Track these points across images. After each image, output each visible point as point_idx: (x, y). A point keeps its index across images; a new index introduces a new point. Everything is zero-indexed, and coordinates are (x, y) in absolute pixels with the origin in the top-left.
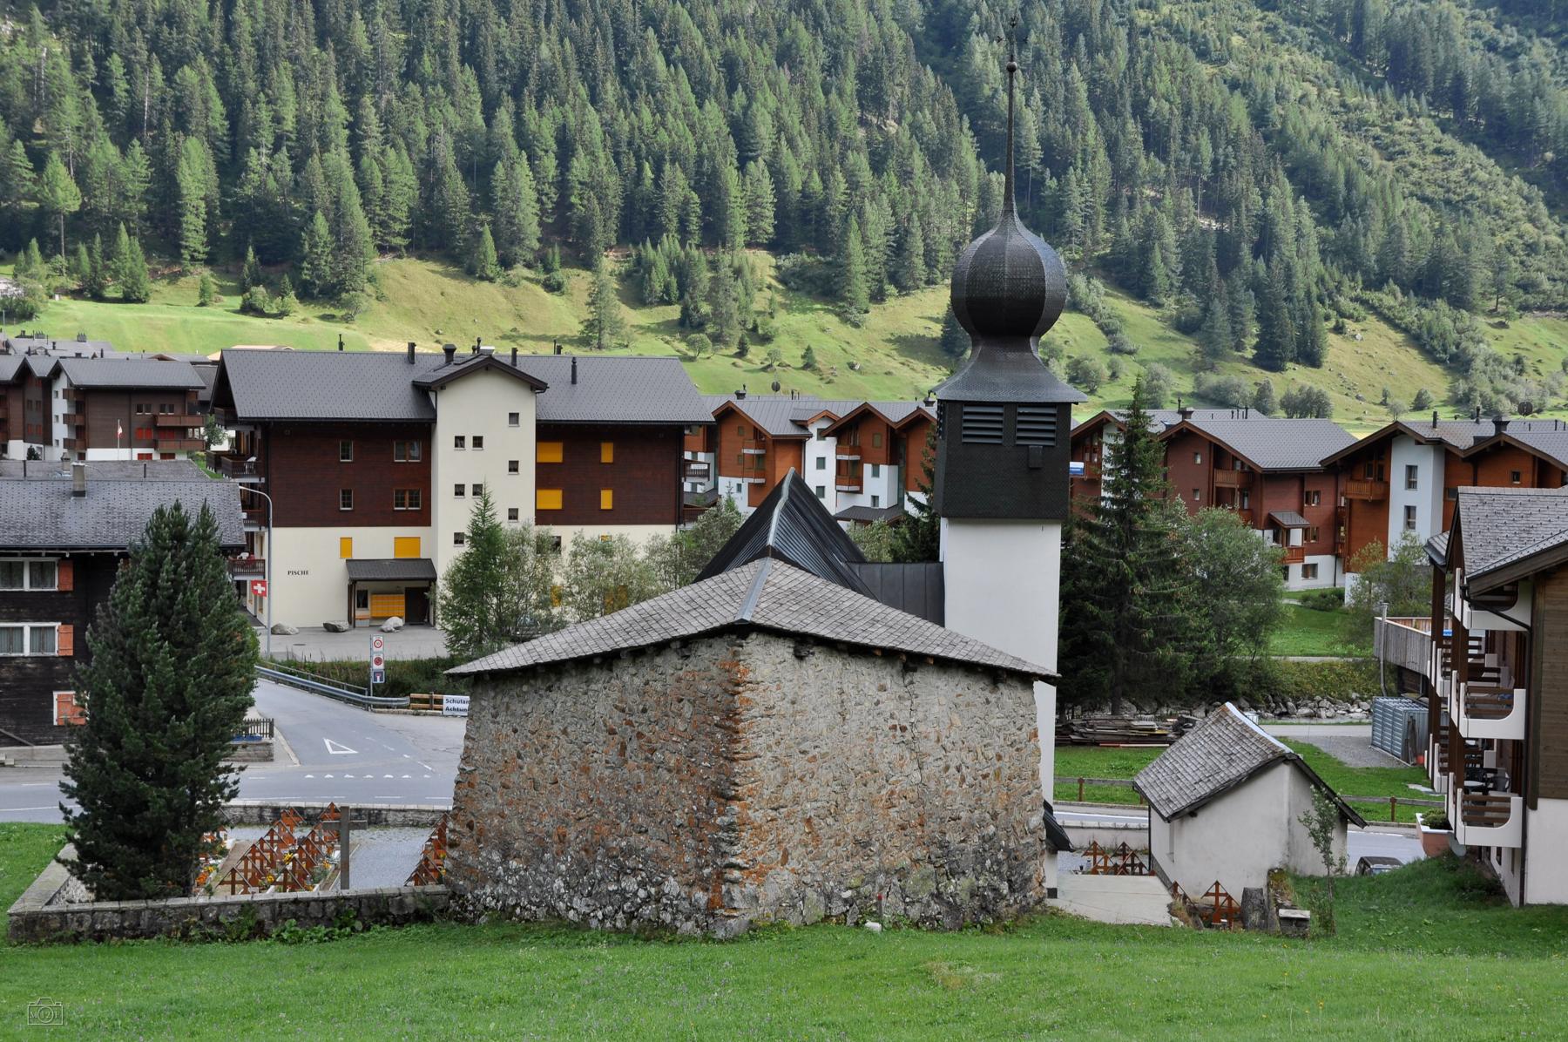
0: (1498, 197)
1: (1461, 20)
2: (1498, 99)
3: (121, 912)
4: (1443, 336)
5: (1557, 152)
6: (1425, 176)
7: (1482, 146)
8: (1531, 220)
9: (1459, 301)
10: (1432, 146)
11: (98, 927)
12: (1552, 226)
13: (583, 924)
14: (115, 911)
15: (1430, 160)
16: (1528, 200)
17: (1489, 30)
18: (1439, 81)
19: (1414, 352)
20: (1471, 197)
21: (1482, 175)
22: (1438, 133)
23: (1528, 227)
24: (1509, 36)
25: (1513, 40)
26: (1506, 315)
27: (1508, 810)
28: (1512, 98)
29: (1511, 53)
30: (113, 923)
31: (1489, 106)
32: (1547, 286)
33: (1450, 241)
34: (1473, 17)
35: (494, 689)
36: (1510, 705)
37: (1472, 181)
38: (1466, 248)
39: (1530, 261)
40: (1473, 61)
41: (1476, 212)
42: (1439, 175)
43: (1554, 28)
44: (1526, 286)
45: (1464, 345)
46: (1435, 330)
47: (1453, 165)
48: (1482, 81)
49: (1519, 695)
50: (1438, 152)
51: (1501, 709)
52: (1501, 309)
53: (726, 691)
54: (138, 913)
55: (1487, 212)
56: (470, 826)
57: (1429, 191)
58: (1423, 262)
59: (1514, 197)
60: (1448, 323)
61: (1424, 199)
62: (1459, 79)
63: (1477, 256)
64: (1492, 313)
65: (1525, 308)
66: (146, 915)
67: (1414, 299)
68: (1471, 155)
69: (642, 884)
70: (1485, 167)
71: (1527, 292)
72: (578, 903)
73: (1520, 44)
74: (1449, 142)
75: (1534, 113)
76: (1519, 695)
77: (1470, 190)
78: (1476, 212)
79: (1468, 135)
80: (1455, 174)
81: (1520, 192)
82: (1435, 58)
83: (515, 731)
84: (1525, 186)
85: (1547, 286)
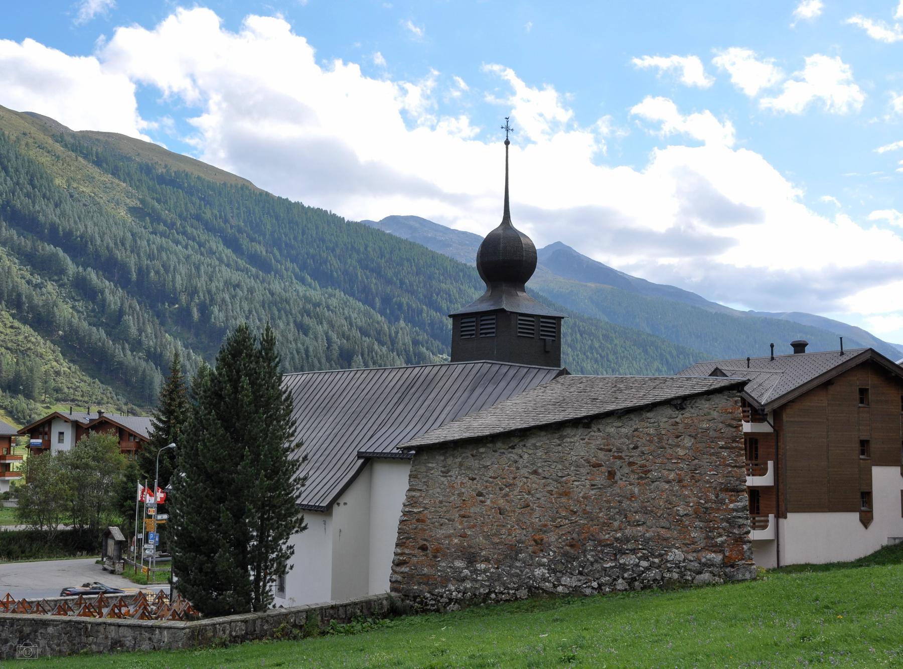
0: (41, 350)
1: (15, 270)
2: (37, 306)
3: (245, 621)
4: (23, 412)
5: (64, 331)
6: (7, 337)
7: (31, 326)
8: (56, 361)
9: (29, 396)
10: (9, 325)
11: (234, 634)
12: (65, 364)
13: (576, 593)
14: (242, 621)
15: (8, 331)
16: (54, 352)
17: (28, 276)
18: (10, 295)
19: (10, 419)
20: (29, 349)
21: (33, 340)
22: (11, 319)
23: (55, 364)
24: (37, 279)
25: (39, 281)
26: (50, 403)
27: (768, 521)
28: (43, 306)
29: (37, 286)
30: (241, 630)
31: (33, 308)
32: (66, 390)
33: (22, 368)
34: (20, 269)
35: (444, 454)
36: (767, 470)
37: (29, 341)
38: (31, 371)
39: (58, 379)
40: (24, 287)
41: (33, 357)
42: (13, 338)
43: (56, 278)
44: (58, 390)
45: (33, 416)
46: (19, 409)
47: (19, 333)
48: (29, 297)
49: (770, 464)
50: (12, 327)
51: (763, 472)
52: (47, 400)
53: (730, 425)
54: (254, 621)
55: (37, 356)
56: (424, 548)
57: (9, 345)
58: (11, 377)
59: (48, 350)
60: (24, 405)
61: (7, 348)
62: (19, 295)
63: (36, 375)
64: (43, 402)
65: (57, 400)
66: (259, 622)
67: (8, 394)
68: (27, 329)
69: (644, 557)
70: (36, 337)
71: (57, 393)
72: (566, 580)
73: (42, 283)
74: (16, 324)
75: (54, 313)
76: (770, 464)
77: (29, 346)
78: (33, 357)
79: (24, 321)
80: (21, 338)
81: (50, 348)
82: (7, 285)
83: (473, 479)
84: (52, 346)
85: (66, 390)
